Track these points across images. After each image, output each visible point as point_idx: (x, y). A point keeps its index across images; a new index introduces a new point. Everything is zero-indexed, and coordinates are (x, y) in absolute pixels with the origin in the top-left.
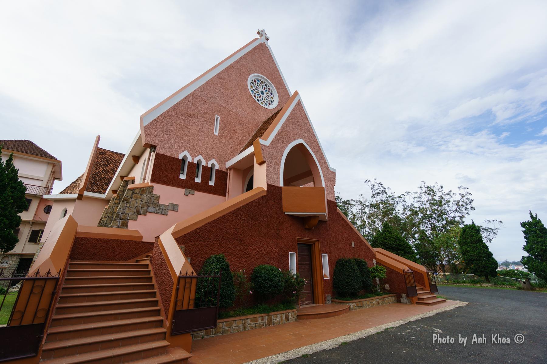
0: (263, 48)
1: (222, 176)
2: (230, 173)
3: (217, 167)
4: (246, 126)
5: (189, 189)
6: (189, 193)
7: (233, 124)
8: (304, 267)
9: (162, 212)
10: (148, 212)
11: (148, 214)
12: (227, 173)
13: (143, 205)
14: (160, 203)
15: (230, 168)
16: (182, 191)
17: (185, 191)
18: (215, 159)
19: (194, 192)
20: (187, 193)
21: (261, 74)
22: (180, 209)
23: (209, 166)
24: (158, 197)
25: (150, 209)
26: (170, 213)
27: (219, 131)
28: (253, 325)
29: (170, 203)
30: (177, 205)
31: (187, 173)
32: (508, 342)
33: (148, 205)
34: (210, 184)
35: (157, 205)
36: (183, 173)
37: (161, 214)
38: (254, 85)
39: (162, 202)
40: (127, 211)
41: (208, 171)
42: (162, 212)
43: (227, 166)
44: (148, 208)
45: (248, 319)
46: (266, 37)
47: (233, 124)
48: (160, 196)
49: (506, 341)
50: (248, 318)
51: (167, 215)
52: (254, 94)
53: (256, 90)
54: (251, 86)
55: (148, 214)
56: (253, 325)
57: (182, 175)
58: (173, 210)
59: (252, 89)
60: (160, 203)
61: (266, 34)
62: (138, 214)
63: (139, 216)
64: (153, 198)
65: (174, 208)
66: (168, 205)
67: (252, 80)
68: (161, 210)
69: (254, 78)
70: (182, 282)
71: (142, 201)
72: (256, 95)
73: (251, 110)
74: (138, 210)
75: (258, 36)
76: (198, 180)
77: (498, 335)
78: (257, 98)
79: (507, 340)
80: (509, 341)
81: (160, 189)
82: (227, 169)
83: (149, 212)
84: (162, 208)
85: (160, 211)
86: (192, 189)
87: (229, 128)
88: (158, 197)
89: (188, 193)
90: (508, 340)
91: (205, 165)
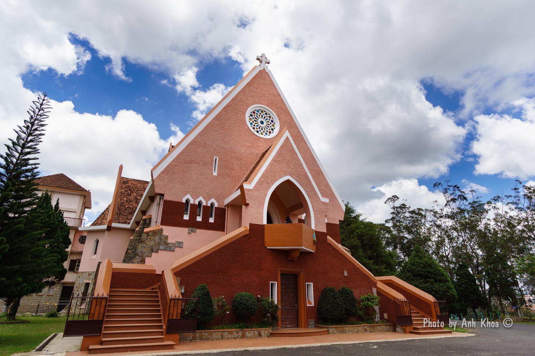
0: (263, 76)
1: (221, 213)
2: (228, 210)
3: (216, 205)
4: (244, 161)
5: (191, 227)
6: (192, 231)
7: (231, 161)
8: (289, 295)
9: (170, 249)
10: (159, 250)
11: (159, 251)
12: (225, 209)
13: (155, 244)
14: (168, 242)
15: (228, 205)
16: (186, 230)
17: (188, 230)
18: (214, 198)
19: (196, 230)
20: (190, 231)
21: (260, 104)
22: (185, 245)
23: (209, 205)
24: (167, 237)
25: (161, 247)
26: (177, 249)
27: (218, 171)
28: (229, 337)
29: (176, 241)
30: (182, 243)
31: (190, 214)
32: (497, 326)
33: (159, 244)
34: (210, 222)
35: (166, 244)
36: (187, 214)
37: (170, 251)
38: (253, 117)
39: (170, 241)
40: (144, 250)
41: (208, 211)
42: (170, 249)
43: (225, 204)
44: (159, 247)
45: (225, 331)
46: (266, 62)
47: (231, 161)
48: (168, 236)
49: (495, 324)
50: (225, 331)
51: (174, 251)
52: (253, 126)
53: (255, 122)
54: (250, 119)
55: (159, 251)
56: (229, 337)
57: (186, 215)
58: (179, 247)
59: (251, 122)
60: (168, 242)
61: (266, 58)
62: (152, 252)
63: (153, 254)
64: (163, 238)
65: (180, 245)
66: (175, 243)
67: (251, 113)
68: (169, 248)
69: (253, 110)
70: (172, 302)
71: (154, 241)
72: (255, 127)
73: (249, 145)
74: (152, 249)
75: (258, 63)
76: (199, 219)
77: (487, 319)
78: (256, 130)
79: (496, 323)
80: (498, 325)
81: (168, 231)
82: (225, 206)
83: (161, 250)
84: (170, 245)
85: (169, 248)
86: (194, 227)
87: (227, 166)
88: (167, 237)
89: (191, 231)
90: (497, 324)
91: (205, 205)
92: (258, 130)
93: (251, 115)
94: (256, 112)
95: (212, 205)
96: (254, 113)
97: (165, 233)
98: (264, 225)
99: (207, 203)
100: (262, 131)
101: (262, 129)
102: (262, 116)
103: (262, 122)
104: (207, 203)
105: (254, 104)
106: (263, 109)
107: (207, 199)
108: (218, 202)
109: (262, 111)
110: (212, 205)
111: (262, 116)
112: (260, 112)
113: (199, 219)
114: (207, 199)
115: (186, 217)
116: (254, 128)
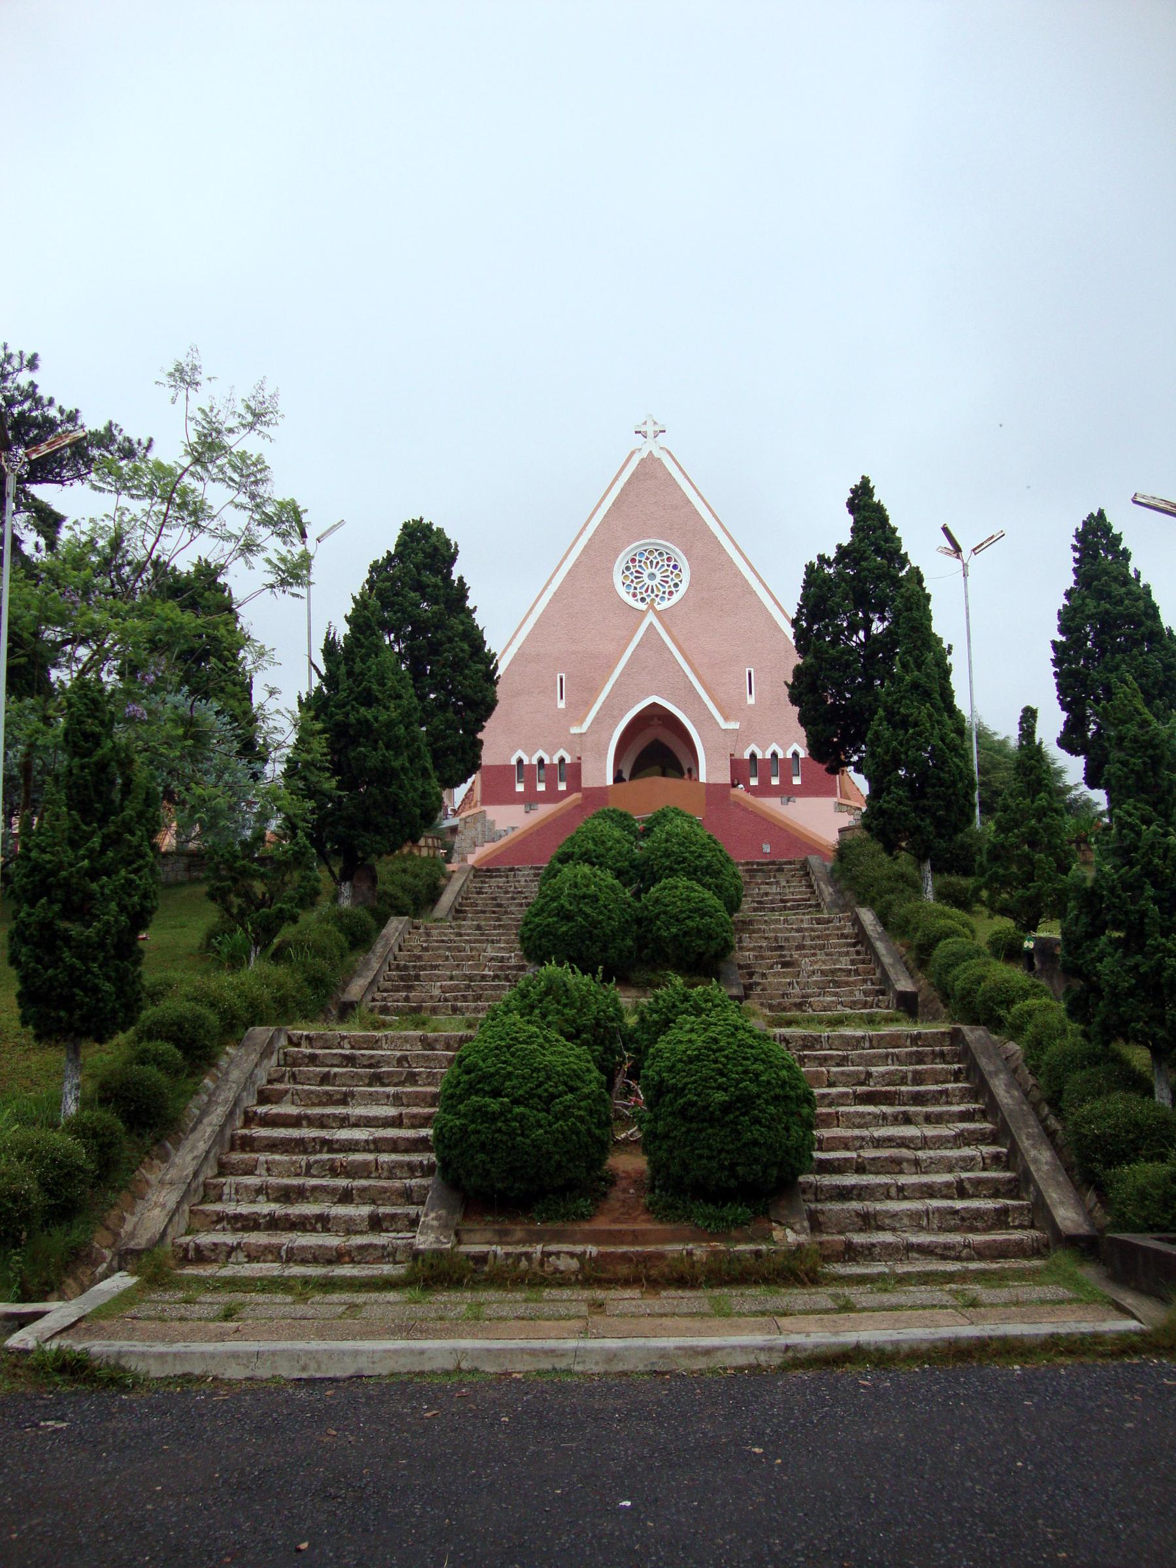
24: (493, 823)
88: (493, 823)
92: (644, 595)
93: (628, 568)
94: (637, 558)
95: (562, 760)
96: (633, 560)
97: (490, 817)
98: (607, 787)
99: (551, 759)
100: (653, 596)
101: (652, 591)
102: (651, 562)
103: (652, 576)
104: (551, 759)
105: (629, 543)
106: (651, 548)
107: (551, 754)
108: (570, 753)
109: (651, 552)
110: (562, 760)
111: (651, 562)
112: (646, 554)
113: (541, 787)
114: (551, 754)
115: (520, 788)
116: (634, 595)
